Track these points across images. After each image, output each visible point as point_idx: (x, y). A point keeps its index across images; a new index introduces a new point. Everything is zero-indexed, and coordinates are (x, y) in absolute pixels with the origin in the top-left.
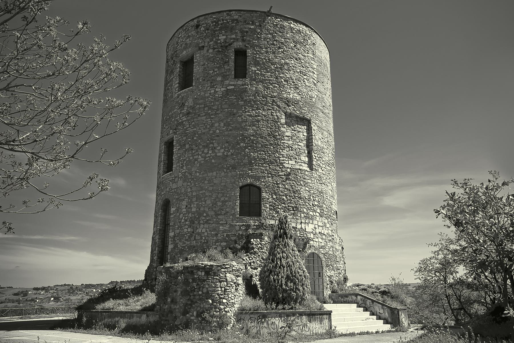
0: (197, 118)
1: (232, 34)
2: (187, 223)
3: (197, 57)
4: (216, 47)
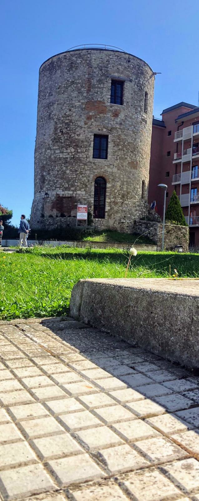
0: (126, 130)
2: (120, 196)
3: (127, 85)
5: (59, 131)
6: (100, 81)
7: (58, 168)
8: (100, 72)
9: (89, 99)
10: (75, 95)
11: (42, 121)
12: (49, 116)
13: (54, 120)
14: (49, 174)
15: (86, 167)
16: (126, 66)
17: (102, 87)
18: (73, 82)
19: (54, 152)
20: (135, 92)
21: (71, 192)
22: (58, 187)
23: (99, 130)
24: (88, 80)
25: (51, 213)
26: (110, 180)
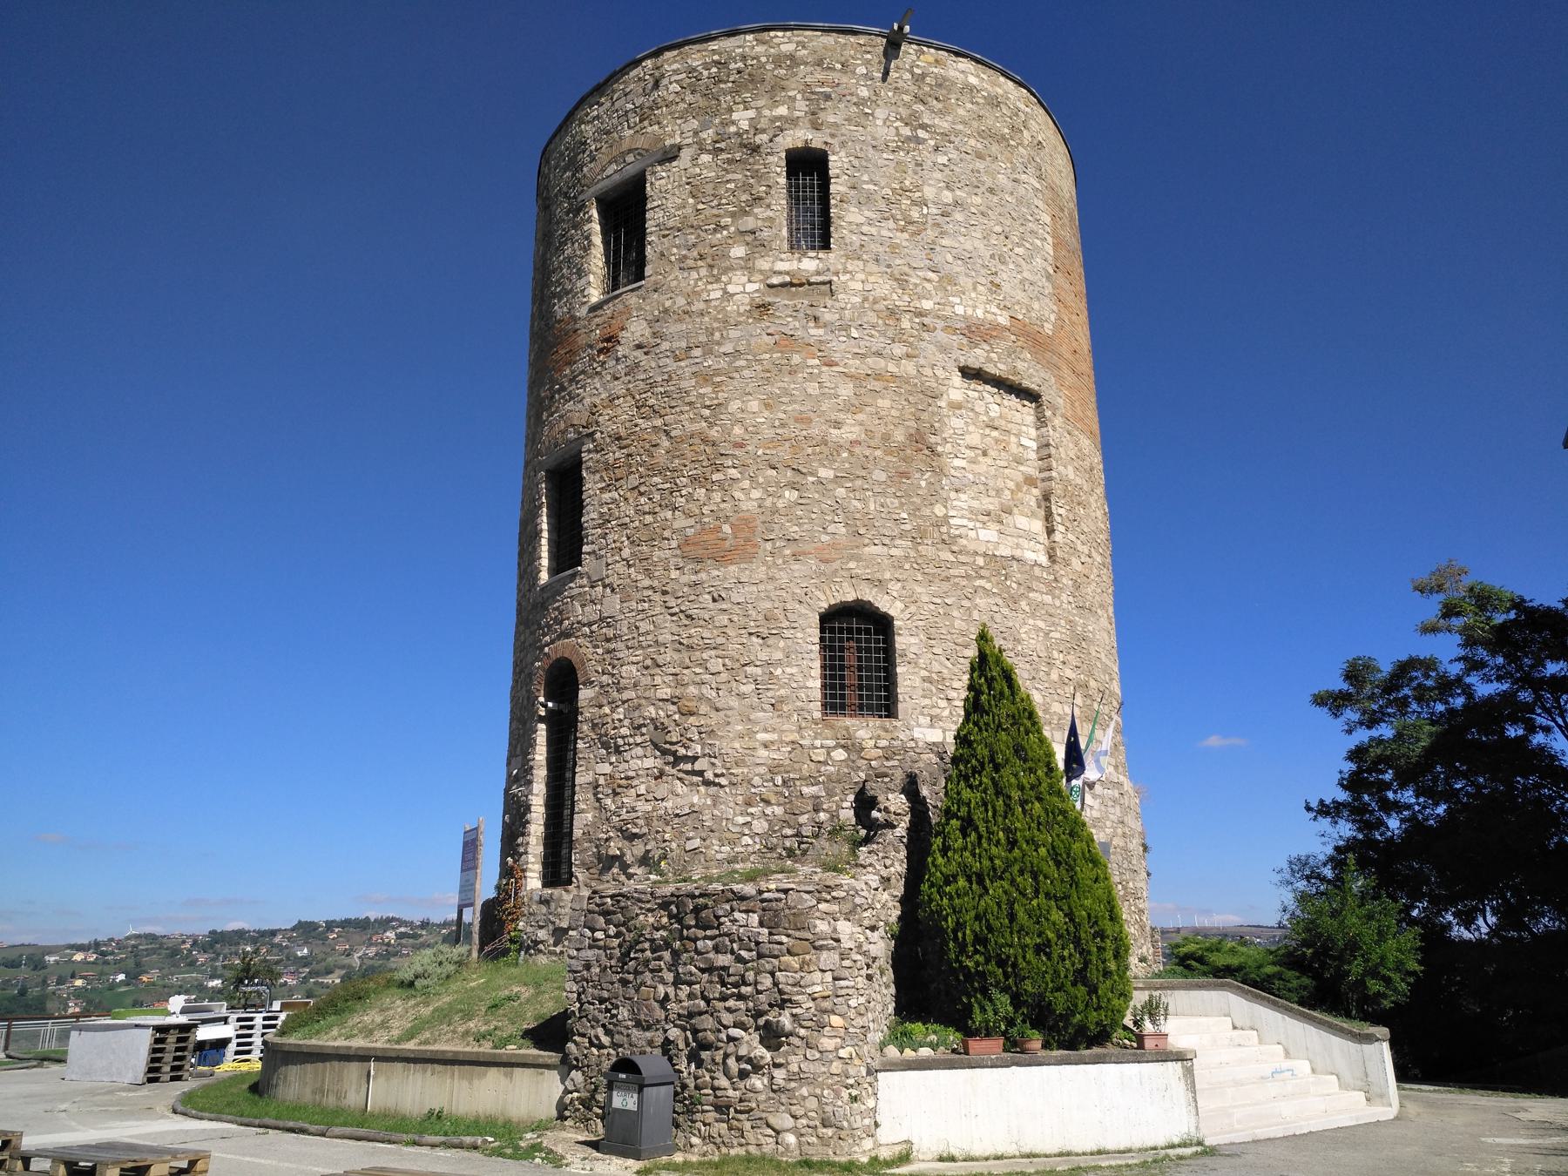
1: (776, 104)
4: (722, 145)
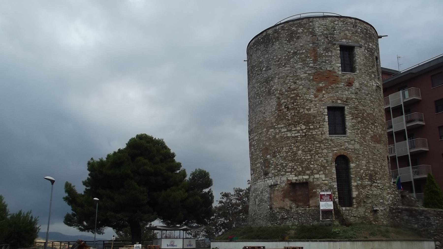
2: (367, 177)
3: (358, 51)
5: (283, 107)
6: (327, 50)
7: (286, 149)
8: (326, 40)
9: (316, 69)
10: (300, 66)
11: (258, 97)
12: (269, 92)
13: (275, 95)
14: (275, 156)
15: (322, 145)
16: (353, 31)
17: (330, 56)
18: (295, 53)
19: (280, 131)
20: (366, 57)
21: (307, 177)
22: (288, 172)
23: (333, 102)
24: (314, 50)
25: (281, 204)
26: (353, 158)
